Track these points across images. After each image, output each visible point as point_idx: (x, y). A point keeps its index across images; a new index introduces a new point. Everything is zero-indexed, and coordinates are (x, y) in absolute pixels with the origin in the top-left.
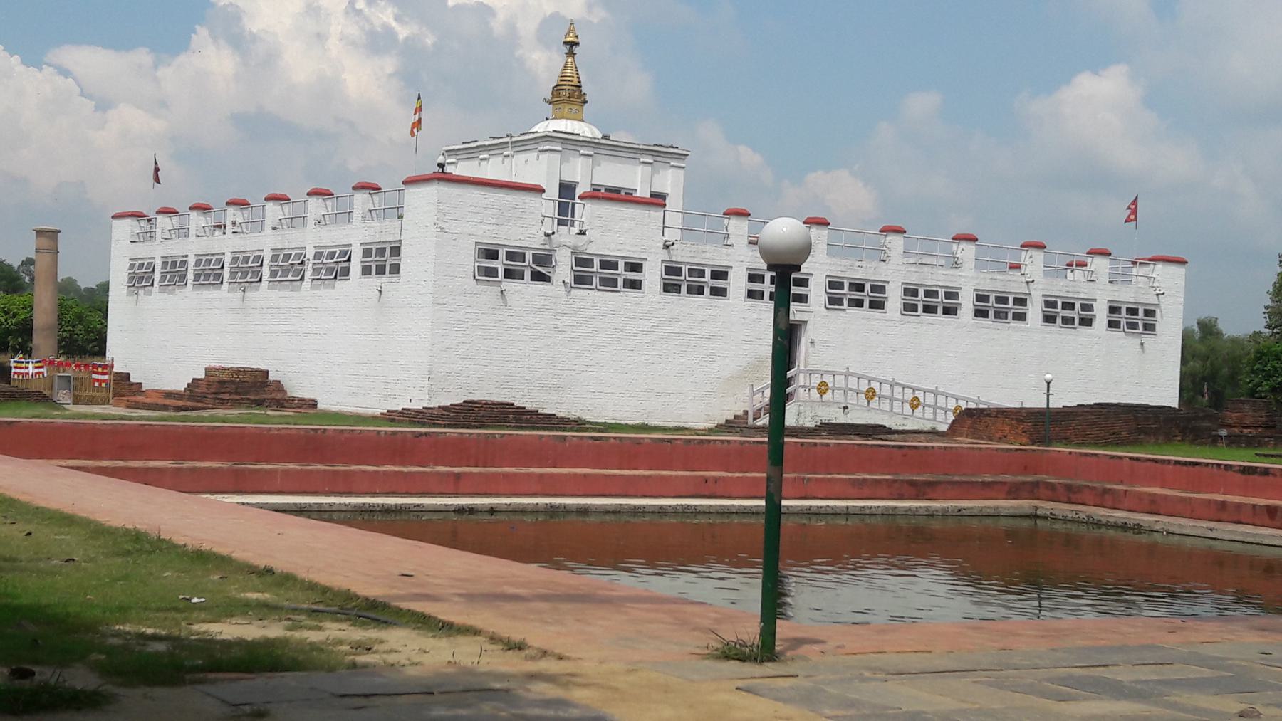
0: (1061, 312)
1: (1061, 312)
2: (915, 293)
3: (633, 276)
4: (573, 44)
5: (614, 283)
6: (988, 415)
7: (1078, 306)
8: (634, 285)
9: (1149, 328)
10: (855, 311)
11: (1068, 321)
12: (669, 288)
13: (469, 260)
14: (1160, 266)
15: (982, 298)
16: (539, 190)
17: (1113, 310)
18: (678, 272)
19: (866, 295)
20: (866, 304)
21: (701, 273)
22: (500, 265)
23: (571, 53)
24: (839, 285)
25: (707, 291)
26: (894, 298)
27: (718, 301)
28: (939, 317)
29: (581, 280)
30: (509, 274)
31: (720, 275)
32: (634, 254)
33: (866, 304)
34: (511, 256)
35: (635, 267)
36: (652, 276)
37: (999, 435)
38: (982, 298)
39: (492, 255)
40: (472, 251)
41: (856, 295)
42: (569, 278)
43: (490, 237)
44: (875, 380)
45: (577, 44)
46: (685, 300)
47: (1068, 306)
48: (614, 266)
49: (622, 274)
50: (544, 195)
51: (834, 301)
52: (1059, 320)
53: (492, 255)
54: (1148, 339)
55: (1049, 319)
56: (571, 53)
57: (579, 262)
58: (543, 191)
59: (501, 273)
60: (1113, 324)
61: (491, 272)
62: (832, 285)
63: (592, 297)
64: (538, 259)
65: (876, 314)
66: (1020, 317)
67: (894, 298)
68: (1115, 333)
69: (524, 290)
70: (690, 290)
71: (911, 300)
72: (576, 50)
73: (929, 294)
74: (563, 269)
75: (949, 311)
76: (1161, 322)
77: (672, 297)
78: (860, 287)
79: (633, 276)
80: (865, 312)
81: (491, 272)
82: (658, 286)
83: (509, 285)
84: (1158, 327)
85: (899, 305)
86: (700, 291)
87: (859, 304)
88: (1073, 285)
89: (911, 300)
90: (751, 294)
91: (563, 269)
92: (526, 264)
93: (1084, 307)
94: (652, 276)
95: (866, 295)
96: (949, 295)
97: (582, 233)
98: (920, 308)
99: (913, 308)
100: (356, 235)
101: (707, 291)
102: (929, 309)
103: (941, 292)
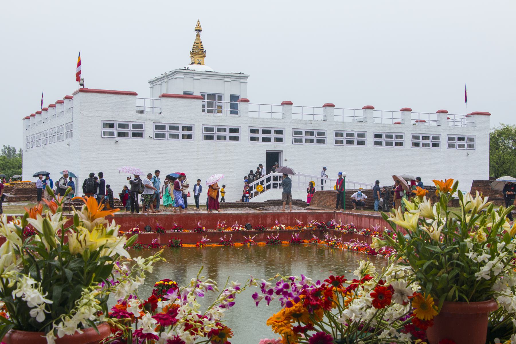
0: (421, 141)
1: (421, 141)
2: (342, 135)
3: (187, 133)
4: (198, 30)
5: (176, 136)
6: (324, 194)
7: (431, 138)
8: (190, 137)
9: (471, 146)
10: (309, 145)
11: (424, 145)
12: (209, 138)
13: (100, 129)
14: (476, 116)
15: (378, 136)
16: (135, 94)
17: (450, 139)
18: (212, 130)
19: (315, 137)
20: (315, 141)
21: (225, 130)
23: (198, 35)
24: (300, 133)
25: (228, 138)
27: (235, 142)
28: (355, 146)
30: (120, 134)
31: (234, 130)
32: (188, 123)
33: (315, 141)
34: (121, 126)
35: (190, 129)
36: (198, 133)
37: (328, 204)
39: (112, 126)
40: (101, 125)
41: (309, 137)
42: (153, 135)
43: (110, 119)
44: (314, 177)
45: (201, 31)
47: (425, 138)
48: (177, 128)
49: (181, 132)
50: (137, 96)
51: (297, 141)
52: (421, 145)
53: (112, 126)
54: (471, 151)
55: (416, 145)
56: (198, 35)
57: (158, 127)
58: (136, 94)
59: (116, 134)
60: (450, 146)
61: (112, 134)
62: (296, 133)
63: (168, 143)
64: (135, 126)
65: (321, 145)
66: (401, 144)
67: (330, 138)
68: (452, 150)
70: (219, 138)
71: (339, 138)
72: (201, 33)
73: (349, 135)
74: (149, 130)
75: (361, 143)
76: (477, 143)
77: (210, 141)
78: (312, 134)
79: (187, 133)
80: (315, 145)
81: (112, 134)
82: (201, 137)
83: (121, 139)
86: (225, 138)
87: (312, 141)
88: (430, 128)
89: (339, 138)
90: (253, 139)
91: (149, 130)
92: (129, 129)
93: (434, 138)
94: (198, 133)
95: (315, 137)
96: (360, 135)
97: (160, 113)
98: (345, 142)
99: (341, 142)
100: (63, 120)
101: (228, 138)
102: (350, 142)
103: (356, 135)
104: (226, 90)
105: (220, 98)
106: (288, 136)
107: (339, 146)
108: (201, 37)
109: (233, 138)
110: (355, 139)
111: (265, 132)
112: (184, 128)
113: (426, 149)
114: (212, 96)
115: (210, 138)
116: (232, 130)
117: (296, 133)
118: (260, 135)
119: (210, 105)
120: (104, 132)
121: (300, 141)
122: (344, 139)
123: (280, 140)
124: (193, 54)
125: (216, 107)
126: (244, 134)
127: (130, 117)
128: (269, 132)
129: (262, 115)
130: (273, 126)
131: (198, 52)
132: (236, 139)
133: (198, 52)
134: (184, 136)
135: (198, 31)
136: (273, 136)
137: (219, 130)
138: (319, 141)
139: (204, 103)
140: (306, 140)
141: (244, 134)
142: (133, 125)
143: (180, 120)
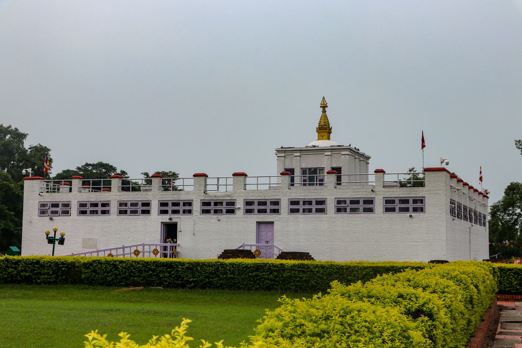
2: (345, 202)
3: (187, 208)
26: (331, 206)
38: (388, 202)
41: (307, 207)
79: (187, 208)
87: (310, 211)
104: (325, 163)
112: (184, 204)
115: (207, 212)
118: (256, 207)
119: (311, 179)
125: (318, 180)
129: (261, 187)
134: (184, 212)
135: (324, 107)
137: (216, 204)
139: (305, 178)
142: (131, 203)
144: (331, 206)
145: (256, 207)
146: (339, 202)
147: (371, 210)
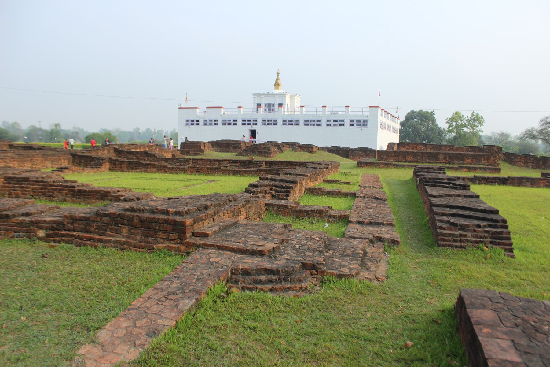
0: (332, 123)
5: (211, 124)
10: (269, 126)
13: (185, 122)
18: (225, 121)
22: (190, 123)
24: (265, 121)
26: (280, 122)
27: (235, 126)
28: (294, 127)
29: (205, 124)
30: (192, 124)
32: (216, 118)
41: (269, 122)
46: (227, 126)
47: (334, 121)
49: (213, 122)
54: (364, 128)
63: (208, 127)
65: (275, 126)
69: (195, 127)
74: (201, 122)
77: (224, 126)
80: (272, 127)
82: (221, 124)
84: (369, 125)
85: (282, 124)
105: (274, 105)
106: (259, 122)
107: (285, 127)
108: (279, 77)
109: (234, 124)
110: (294, 122)
111: (249, 121)
113: (335, 127)
114: (270, 105)
115: (225, 124)
116: (234, 121)
117: (263, 121)
118: (247, 122)
120: (187, 124)
121: (265, 124)
122: (288, 123)
123: (256, 124)
124: (275, 85)
126: (239, 122)
127: (195, 118)
128: (250, 121)
130: (252, 118)
131: (277, 84)
132: (236, 124)
133: (277, 84)
136: (252, 122)
137: (229, 121)
138: (274, 124)
140: (268, 124)
141: (239, 122)
143: (213, 118)
144: (280, 122)
145: (247, 122)
146: (284, 121)
147: (297, 125)
